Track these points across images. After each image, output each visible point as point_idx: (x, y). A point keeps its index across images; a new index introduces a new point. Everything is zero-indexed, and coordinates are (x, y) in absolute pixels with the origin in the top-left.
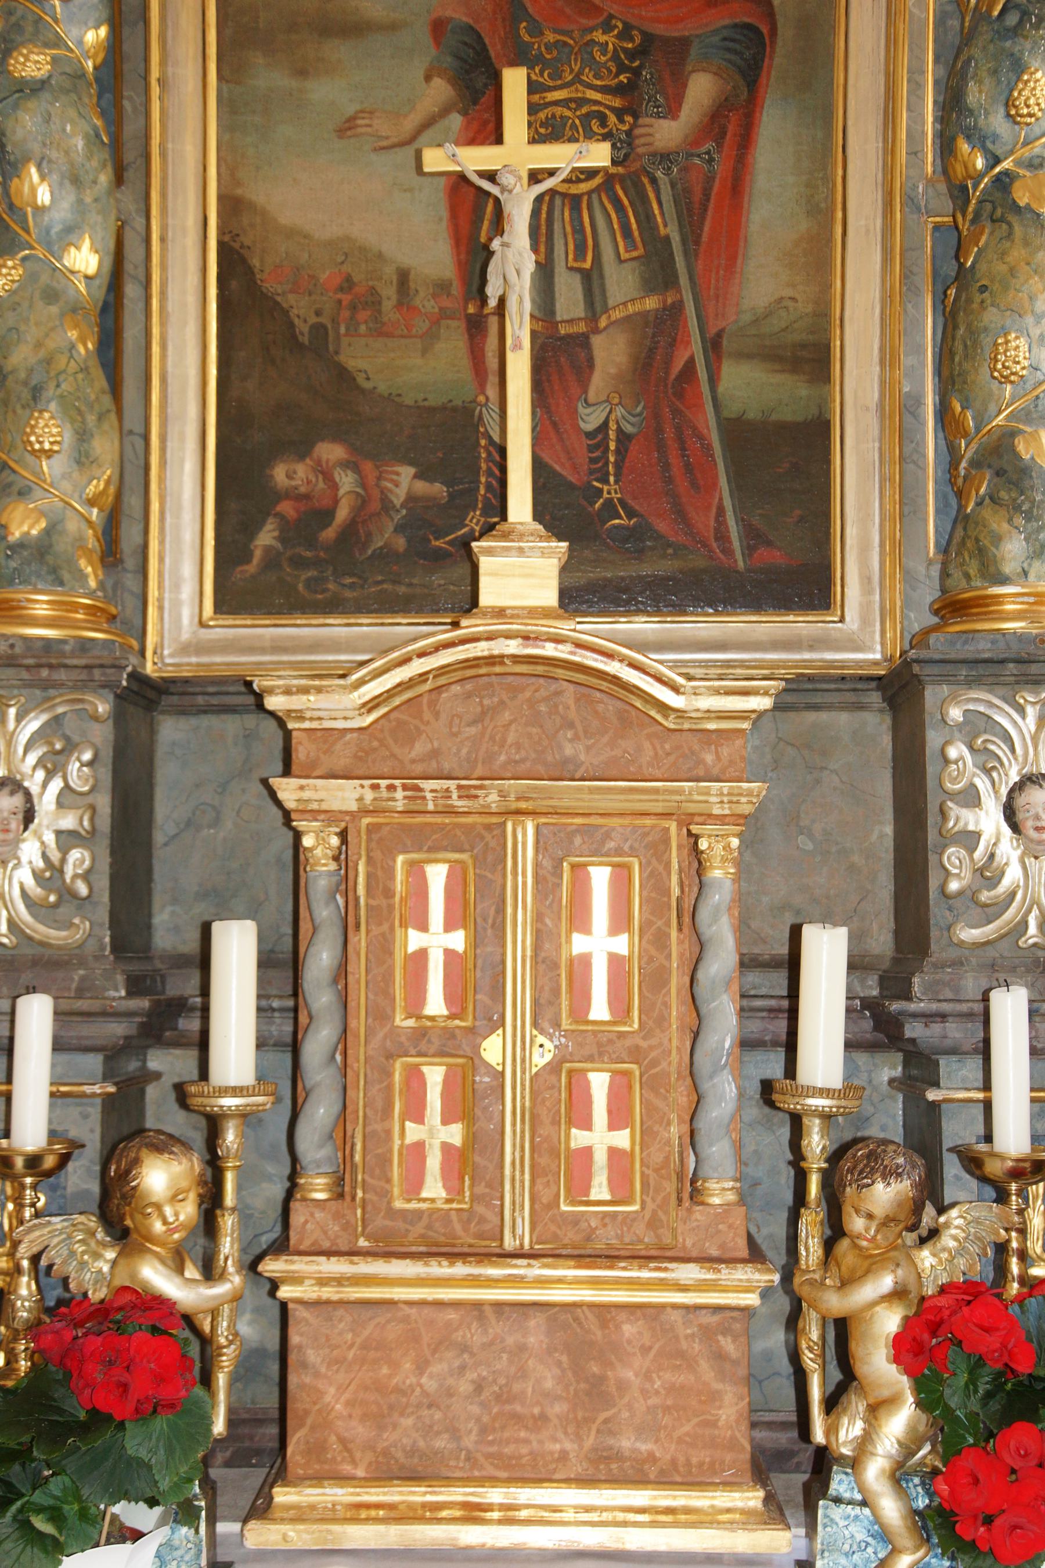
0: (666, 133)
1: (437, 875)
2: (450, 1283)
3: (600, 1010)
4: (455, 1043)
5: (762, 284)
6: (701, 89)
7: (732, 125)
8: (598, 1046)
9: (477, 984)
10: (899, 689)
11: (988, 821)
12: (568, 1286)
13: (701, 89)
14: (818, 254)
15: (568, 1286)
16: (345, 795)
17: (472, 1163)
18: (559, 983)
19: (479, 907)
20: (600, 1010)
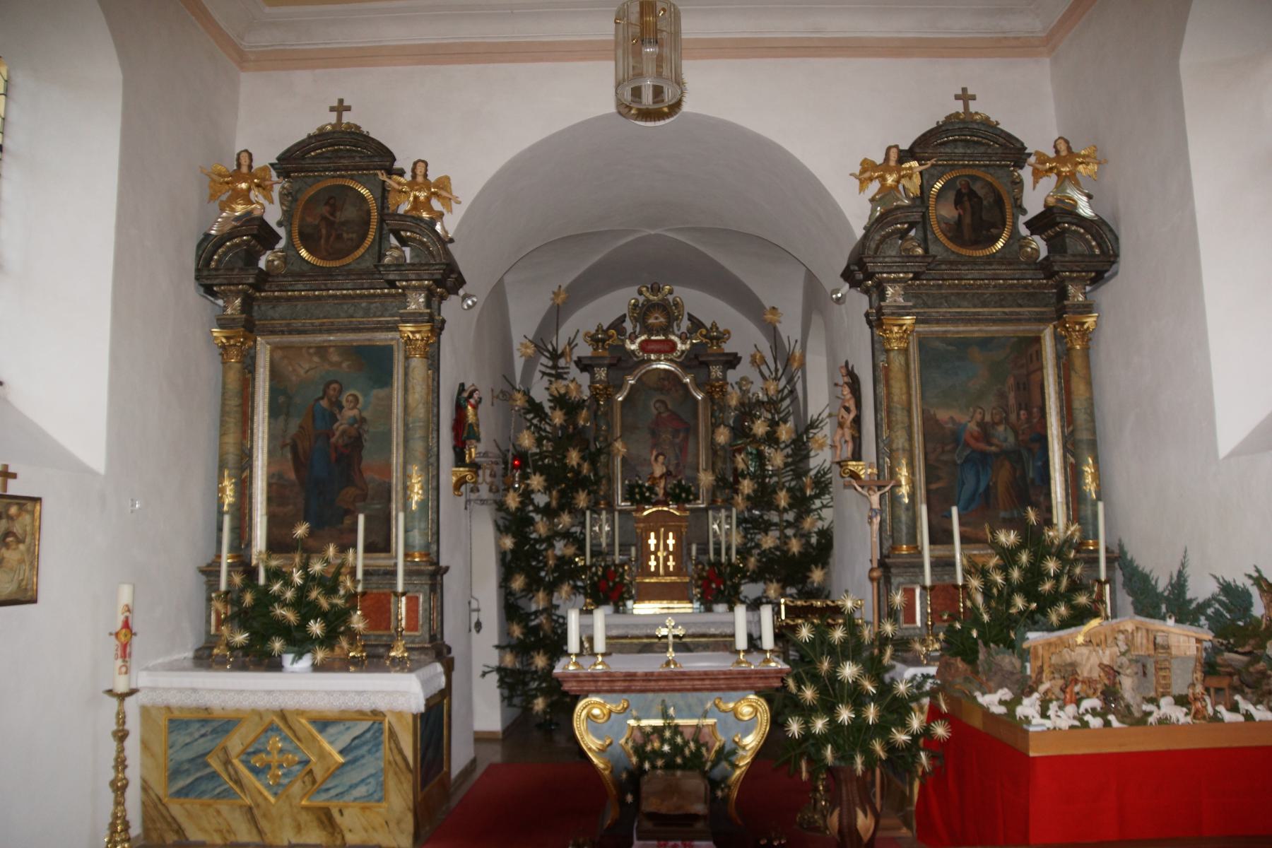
0: (677, 441)
1: (652, 535)
2: (654, 580)
3: (671, 549)
4: (655, 553)
5: (690, 459)
6: (682, 435)
7: (686, 439)
8: (670, 553)
9: (657, 546)
10: (706, 510)
11: (716, 526)
12: (668, 579)
13: (682, 435)
14: (697, 456)
15: (668, 579)
16: (642, 525)
17: (657, 567)
18: (666, 546)
19: (657, 537)
20: (671, 549)
